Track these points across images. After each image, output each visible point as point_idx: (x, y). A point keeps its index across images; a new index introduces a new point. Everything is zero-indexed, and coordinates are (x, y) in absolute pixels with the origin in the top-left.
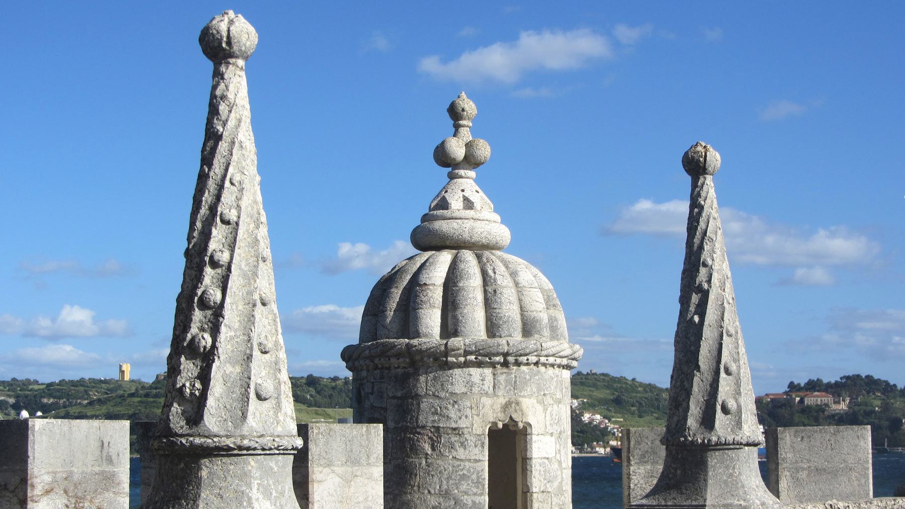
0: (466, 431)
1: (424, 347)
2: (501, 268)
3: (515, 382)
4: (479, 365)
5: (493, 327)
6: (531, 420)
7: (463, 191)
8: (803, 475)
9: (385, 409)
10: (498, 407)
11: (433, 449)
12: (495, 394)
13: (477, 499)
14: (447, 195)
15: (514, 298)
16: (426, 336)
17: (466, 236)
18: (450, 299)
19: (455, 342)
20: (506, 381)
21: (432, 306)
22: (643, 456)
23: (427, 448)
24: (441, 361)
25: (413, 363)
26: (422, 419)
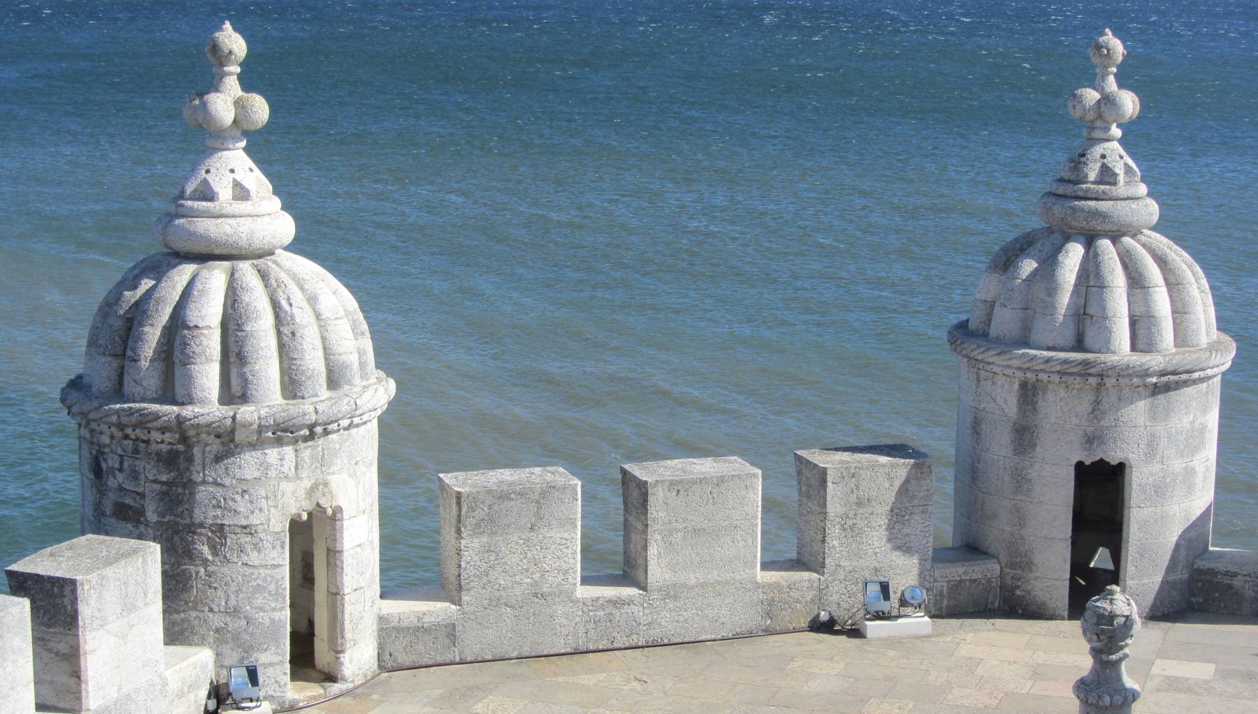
0: (260, 529)
1: (202, 420)
2: (298, 297)
3: (323, 456)
4: (279, 442)
5: (292, 386)
6: (342, 501)
7: (232, 171)
8: (677, 538)
9: (142, 495)
10: (302, 493)
11: (215, 553)
12: (298, 477)
13: (276, 616)
14: (210, 178)
15: (318, 343)
16: (203, 402)
17: (243, 243)
18: (234, 348)
19: (247, 412)
20: (312, 457)
21: (209, 360)
22: (478, 525)
23: (206, 550)
24: (229, 441)
25: (184, 439)
26: (198, 515)
